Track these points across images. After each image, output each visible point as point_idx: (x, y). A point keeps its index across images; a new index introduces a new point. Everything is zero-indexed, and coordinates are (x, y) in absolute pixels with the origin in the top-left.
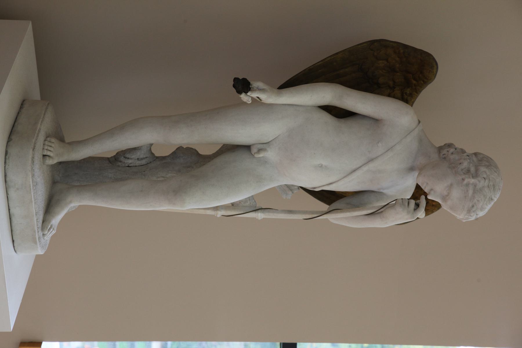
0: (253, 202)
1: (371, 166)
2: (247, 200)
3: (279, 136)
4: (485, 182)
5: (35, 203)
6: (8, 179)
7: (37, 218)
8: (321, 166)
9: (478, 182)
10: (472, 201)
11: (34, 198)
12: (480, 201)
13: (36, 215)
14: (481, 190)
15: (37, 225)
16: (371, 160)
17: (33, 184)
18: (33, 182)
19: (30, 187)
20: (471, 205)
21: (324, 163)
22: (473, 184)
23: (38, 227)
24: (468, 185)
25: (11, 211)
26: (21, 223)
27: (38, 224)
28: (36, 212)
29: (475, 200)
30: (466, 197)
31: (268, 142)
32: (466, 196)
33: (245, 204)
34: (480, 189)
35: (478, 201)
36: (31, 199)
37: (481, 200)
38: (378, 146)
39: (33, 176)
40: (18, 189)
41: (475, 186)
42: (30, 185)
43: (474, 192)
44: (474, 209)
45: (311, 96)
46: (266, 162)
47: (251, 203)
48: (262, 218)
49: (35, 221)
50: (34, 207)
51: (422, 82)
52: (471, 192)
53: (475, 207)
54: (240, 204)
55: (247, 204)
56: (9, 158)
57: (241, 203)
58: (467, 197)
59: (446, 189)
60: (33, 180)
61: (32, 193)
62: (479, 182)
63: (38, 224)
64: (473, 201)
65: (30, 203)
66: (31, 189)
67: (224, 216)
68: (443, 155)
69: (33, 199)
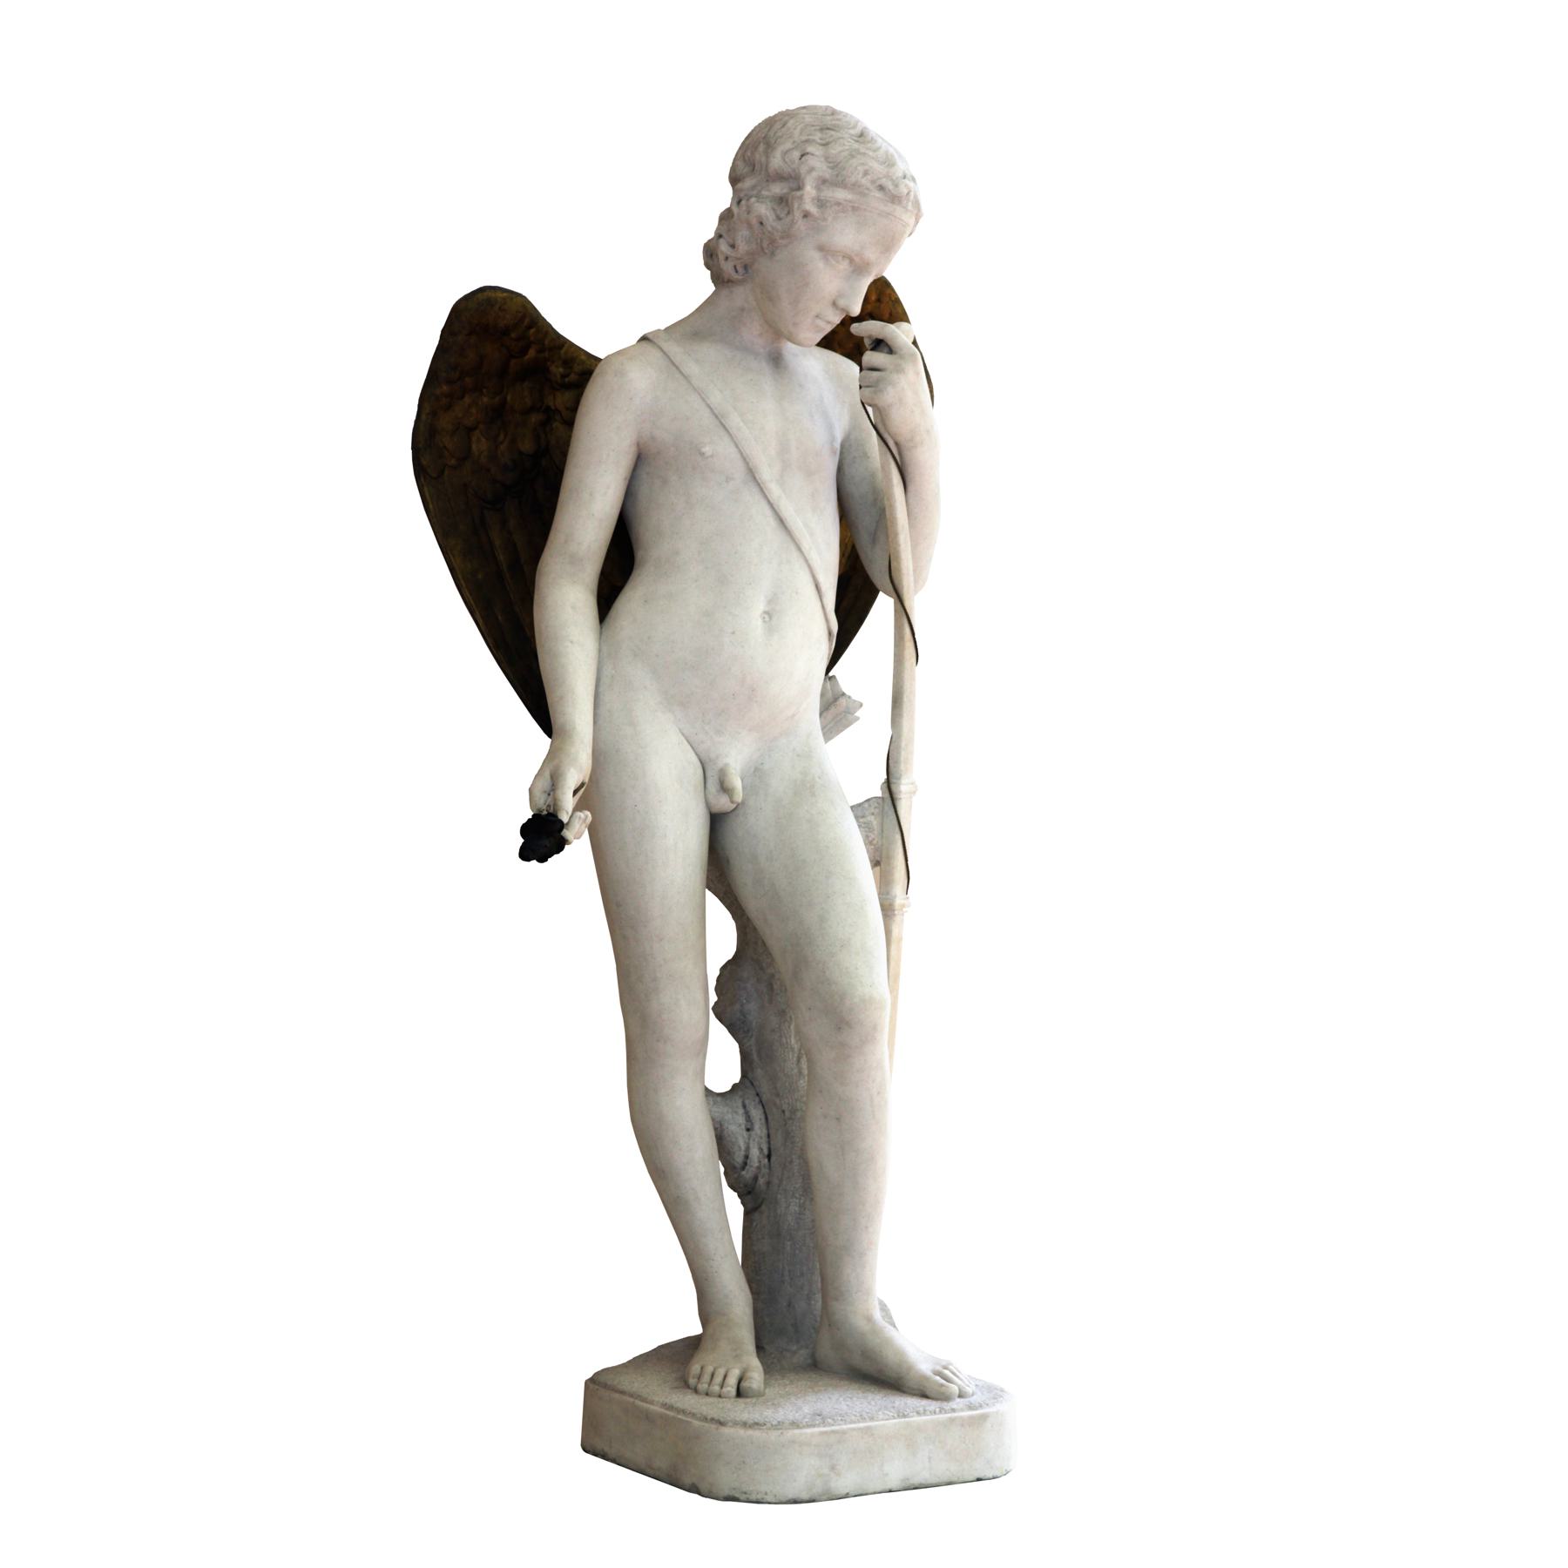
0: (870, 806)
1: (767, 474)
2: (865, 823)
3: (683, 734)
4: (813, 155)
5: (872, 1419)
6: (805, 1496)
7: (915, 1414)
8: (769, 615)
9: (814, 174)
10: (866, 191)
11: (859, 1422)
12: (866, 167)
13: (904, 1416)
15: (935, 1413)
16: (752, 474)
17: (819, 1426)
18: (814, 1426)
19: (826, 1433)
20: (878, 194)
21: (760, 606)
22: (818, 188)
24: (821, 203)
25: (893, 1484)
26: (930, 1458)
28: (898, 1416)
29: (864, 181)
30: (854, 209)
31: (699, 763)
32: (853, 207)
33: (876, 827)
34: (832, 168)
36: (860, 1429)
37: (863, 164)
38: (712, 456)
39: (795, 1425)
40: (833, 1468)
41: (824, 181)
42: (822, 1433)
43: (838, 181)
45: (572, 642)
46: (756, 769)
47: (873, 811)
51: (532, 331)
52: (841, 195)
53: (884, 181)
54: (875, 842)
55: (875, 823)
56: (745, 1493)
57: (874, 839)
58: (856, 205)
59: (834, 263)
60: (808, 1426)
61: (844, 1427)
62: (812, 169)
64: (868, 189)
65: (873, 1435)
66: (833, 1432)
67: (705, 783)
68: (737, 272)
69: (862, 1425)
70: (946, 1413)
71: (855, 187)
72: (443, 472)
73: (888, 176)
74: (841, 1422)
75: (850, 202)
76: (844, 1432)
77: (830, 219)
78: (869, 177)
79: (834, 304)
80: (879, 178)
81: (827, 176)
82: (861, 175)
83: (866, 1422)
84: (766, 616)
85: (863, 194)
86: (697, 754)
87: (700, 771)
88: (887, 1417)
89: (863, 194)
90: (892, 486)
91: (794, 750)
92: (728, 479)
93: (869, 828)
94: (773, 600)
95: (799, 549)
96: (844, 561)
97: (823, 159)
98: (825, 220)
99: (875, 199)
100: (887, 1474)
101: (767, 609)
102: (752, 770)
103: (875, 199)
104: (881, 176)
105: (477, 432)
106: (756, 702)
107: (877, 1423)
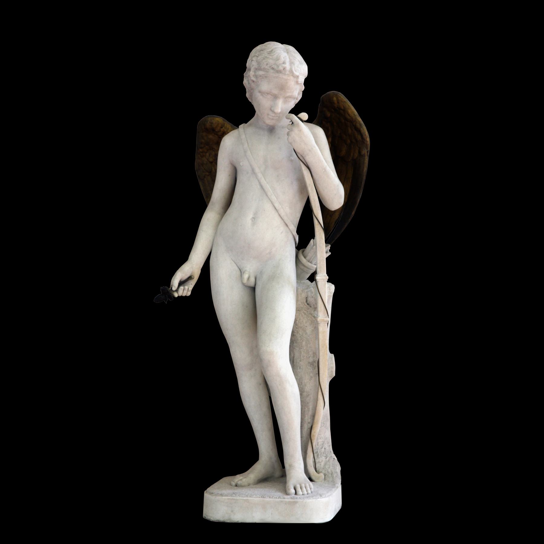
3: (232, 260)
5: (250, 497)
7: (268, 497)
8: (254, 219)
9: (253, 67)
10: (268, 71)
11: (245, 497)
12: (267, 62)
13: (264, 498)
14: (259, 63)
15: (276, 498)
17: (229, 496)
19: (230, 499)
20: (272, 71)
21: (250, 216)
22: (255, 72)
23: (279, 498)
24: (256, 76)
26: (272, 514)
27: (275, 498)
28: (261, 497)
29: (266, 67)
30: (266, 77)
31: (239, 270)
32: (265, 76)
33: (313, 292)
34: (258, 64)
35: (267, 64)
36: (243, 499)
37: (266, 61)
38: (242, 166)
39: (222, 495)
40: (232, 511)
41: (256, 69)
42: (228, 499)
44: (275, 67)
45: (203, 231)
46: (261, 272)
47: (313, 286)
48: (327, 275)
49: (271, 499)
50: (254, 498)
52: (261, 73)
53: (273, 66)
54: (314, 297)
57: (313, 296)
58: (266, 76)
59: (265, 96)
61: (238, 498)
62: (253, 65)
63: (275, 498)
64: (268, 70)
65: (249, 502)
66: (232, 499)
69: (244, 498)
70: (281, 499)
71: (264, 70)
72: (205, 177)
73: (275, 64)
74: (238, 496)
75: (264, 75)
76: (237, 500)
77: (260, 81)
78: (268, 66)
79: (271, 110)
80: (272, 65)
81: (256, 67)
82: (265, 65)
83: (248, 498)
84: (253, 219)
85: (267, 72)
86: (238, 267)
87: (240, 273)
88: (257, 497)
89: (267, 72)
90: (302, 170)
91: (273, 264)
92: (247, 173)
93: (311, 292)
94: (256, 214)
95: (267, 195)
96: (347, 196)
97: (256, 61)
98: (258, 82)
99: (271, 73)
100: (254, 517)
101: (253, 217)
102: (260, 272)
103: (271, 73)
104: (273, 64)
105: (213, 163)
106: (251, 249)
107: (251, 498)
